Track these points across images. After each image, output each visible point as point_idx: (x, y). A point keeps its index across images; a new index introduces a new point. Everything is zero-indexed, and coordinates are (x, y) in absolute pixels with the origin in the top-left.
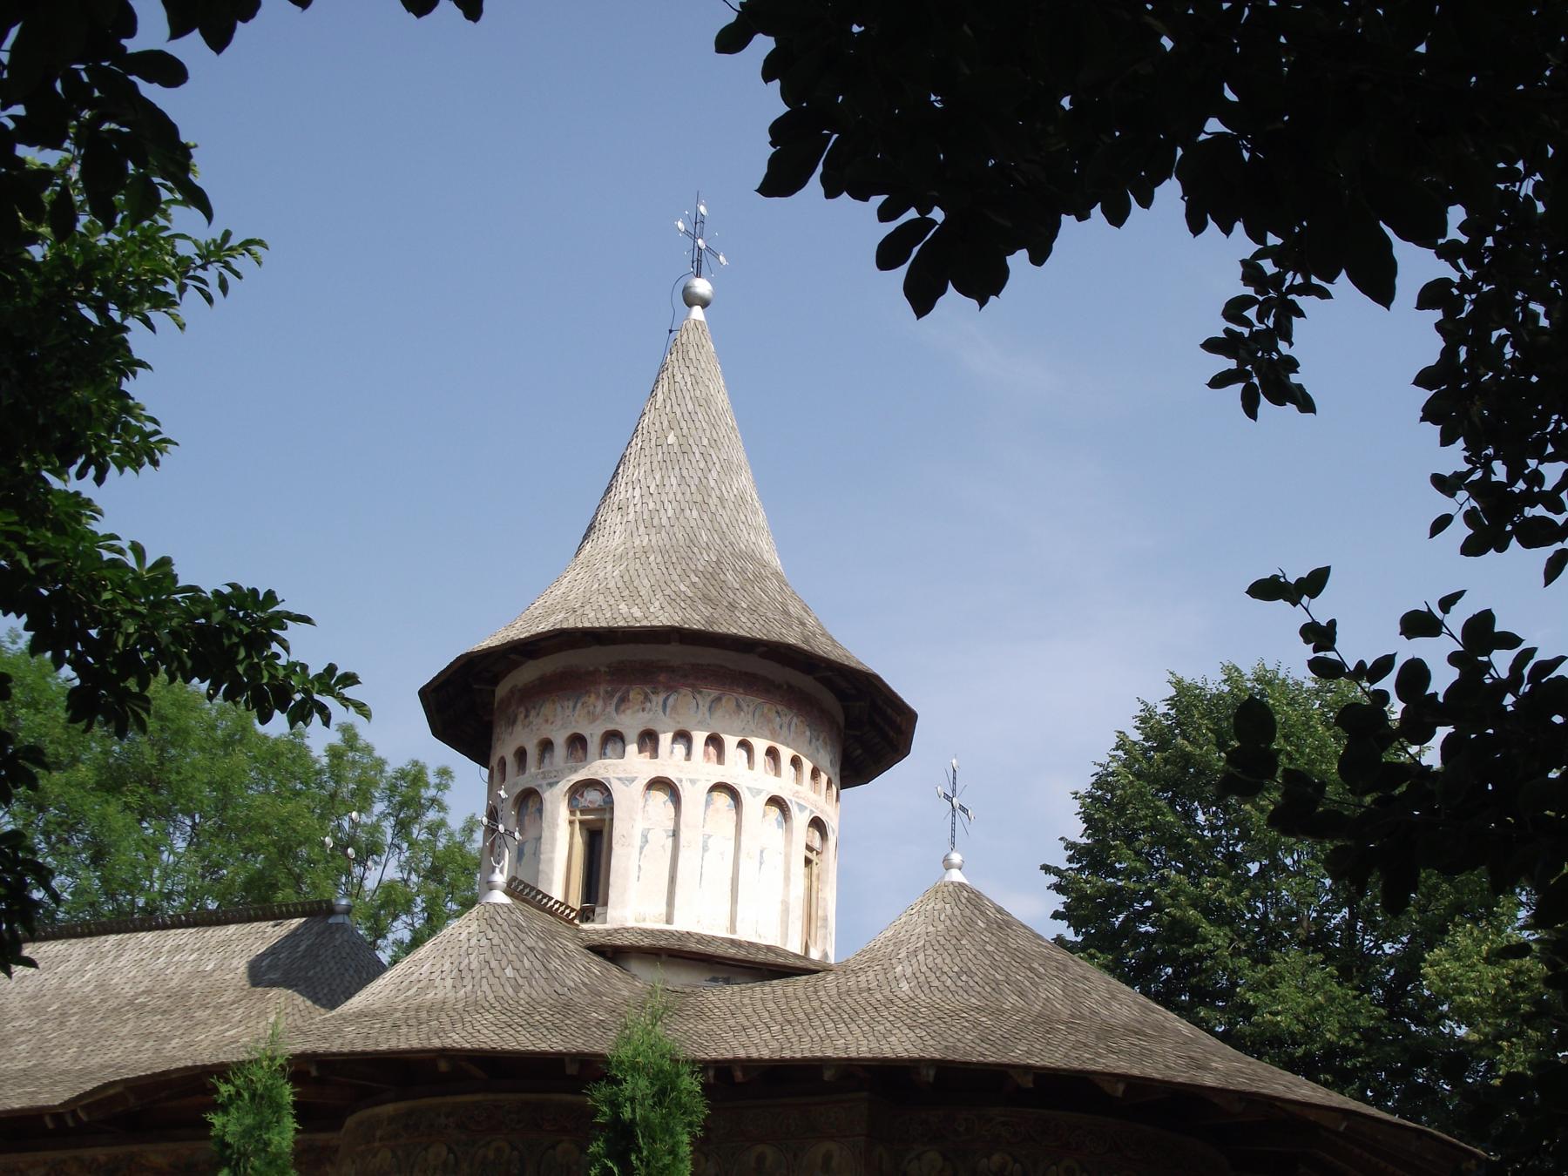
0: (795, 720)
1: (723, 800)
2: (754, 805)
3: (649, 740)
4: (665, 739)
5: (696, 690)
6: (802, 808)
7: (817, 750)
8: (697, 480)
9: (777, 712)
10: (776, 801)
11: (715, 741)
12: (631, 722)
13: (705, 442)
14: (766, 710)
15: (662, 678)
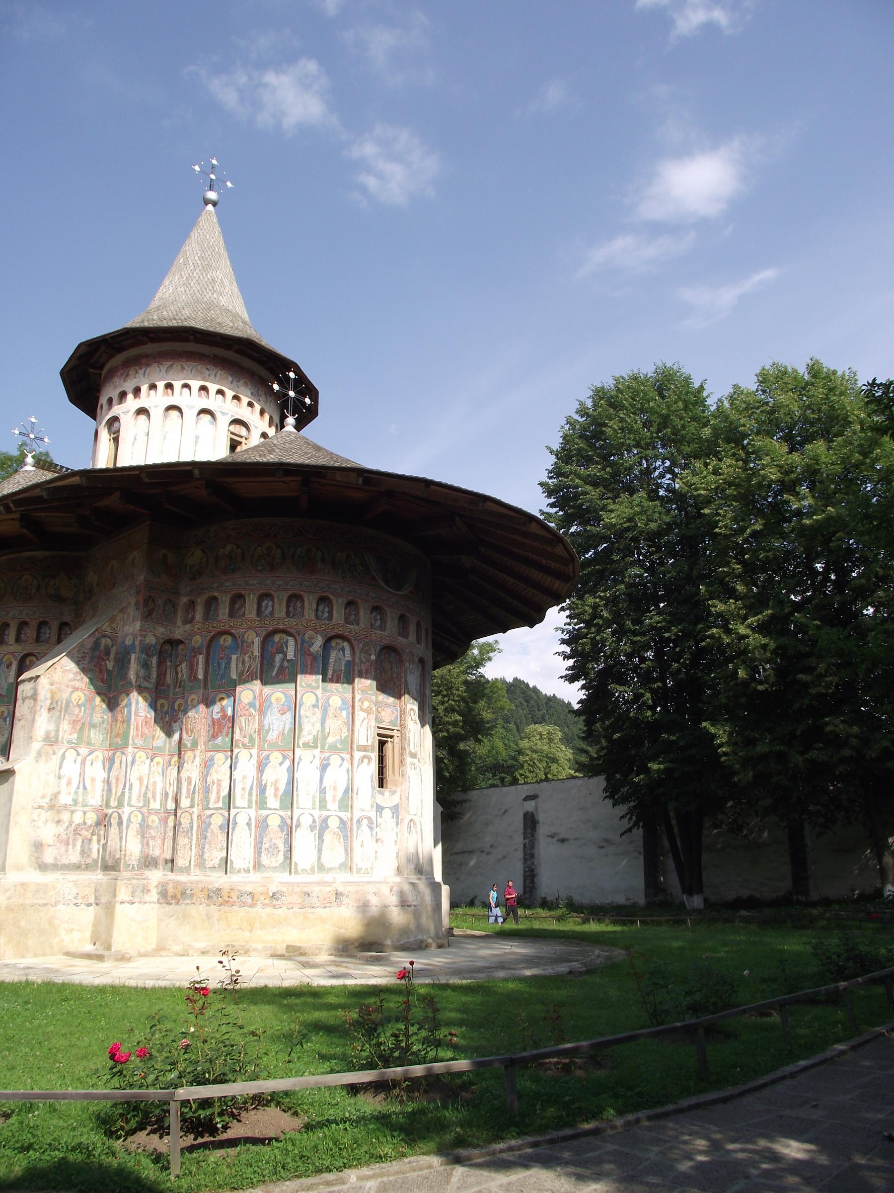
0: (220, 372)
1: (174, 414)
2: (190, 414)
3: (137, 391)
4: (144, 388)
5: (159, 363)
6: (223, 414)
7: (238, 386)
8: (187, 275)
9: (207, 369)
10: (204, 411)
11: (169, 386)
12: (129, 386)
13: (196, 258)
14: (199, 368)
15: (144, 361)
